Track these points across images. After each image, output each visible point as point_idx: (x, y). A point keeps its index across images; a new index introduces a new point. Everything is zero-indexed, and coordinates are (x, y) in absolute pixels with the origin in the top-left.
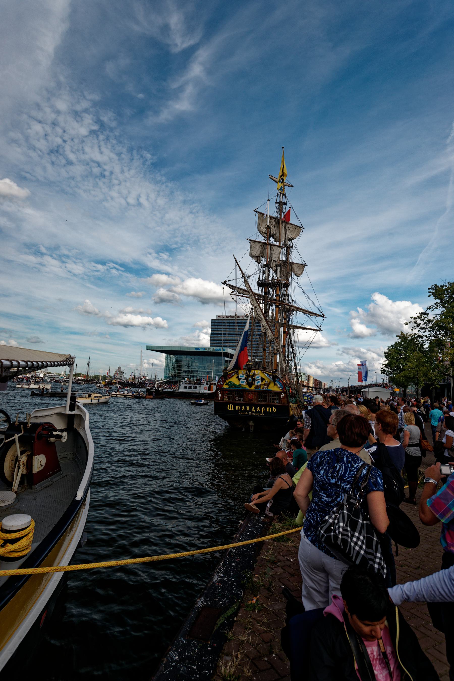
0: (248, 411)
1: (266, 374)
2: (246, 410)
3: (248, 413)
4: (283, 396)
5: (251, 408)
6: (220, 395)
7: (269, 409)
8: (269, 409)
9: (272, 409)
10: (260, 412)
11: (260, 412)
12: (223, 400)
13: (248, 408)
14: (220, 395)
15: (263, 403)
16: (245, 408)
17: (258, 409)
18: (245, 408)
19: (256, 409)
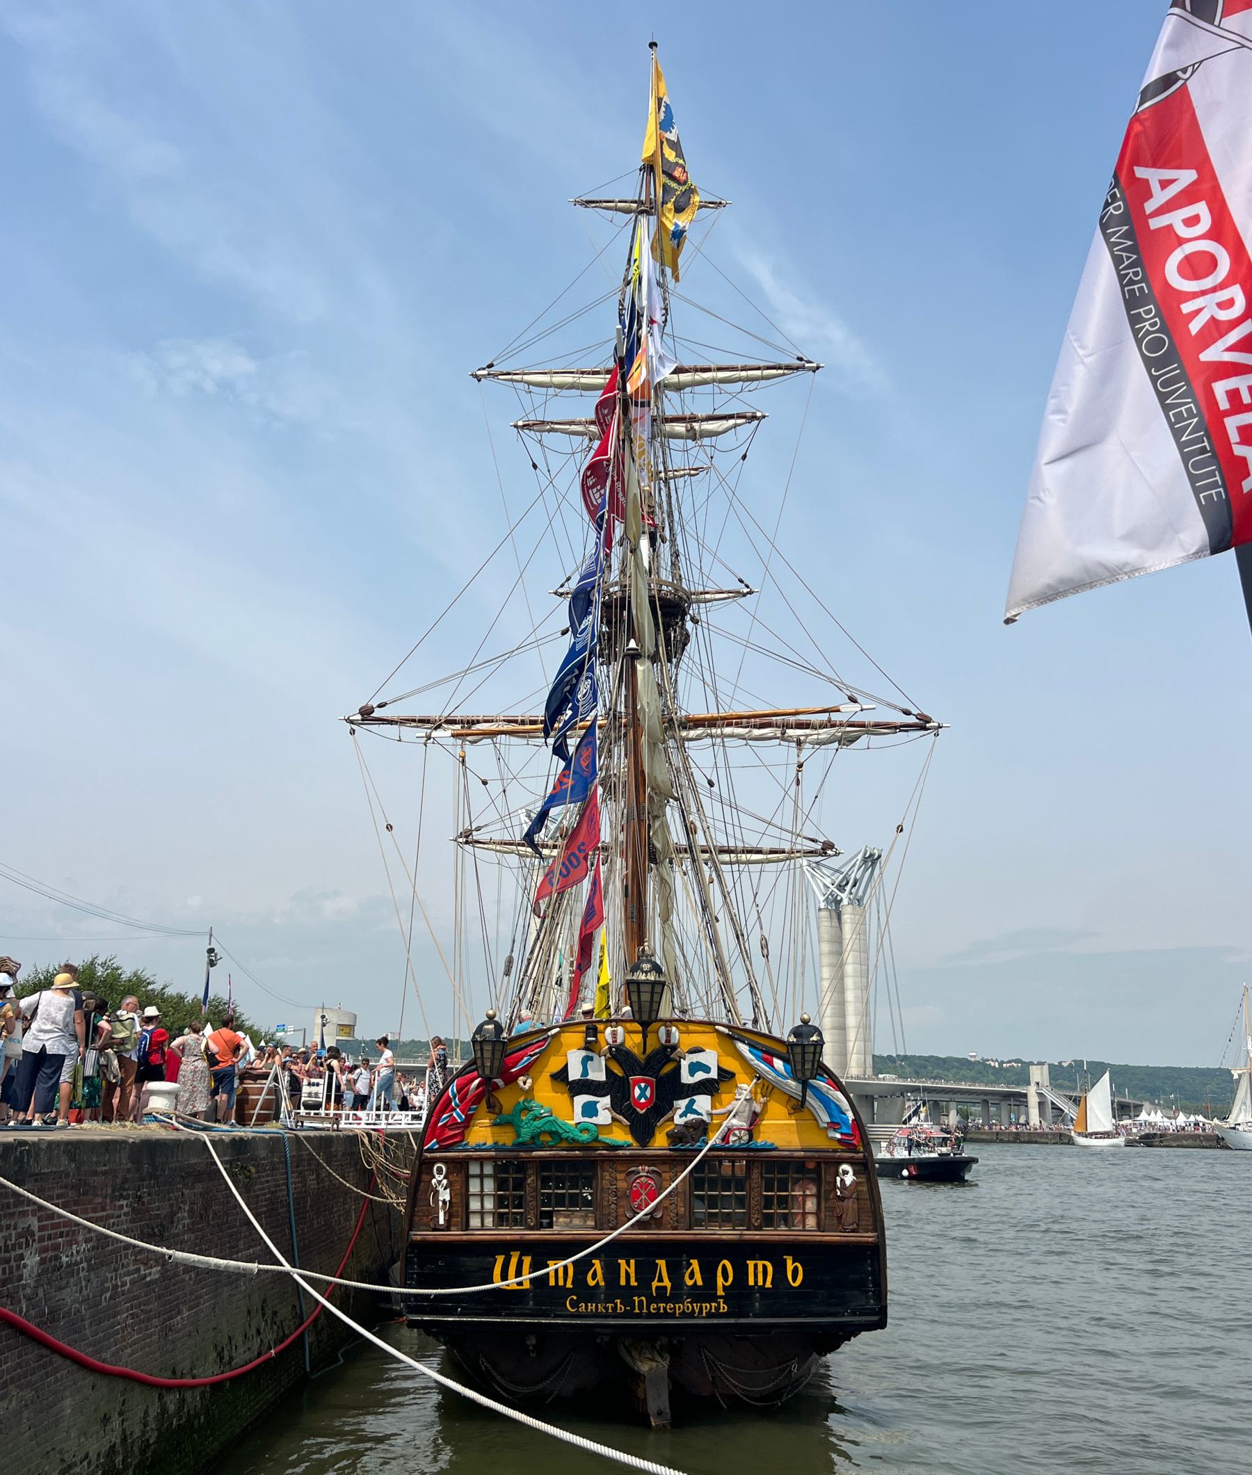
0: (627, 1294)
1: (743, 1048)
2: (613, 1287)
3: (628, 1302)
4: (849, 1179)
5: (646, 1272)
6: (445, 1195)
7: (759, 1273)
8: (759, 1273)
9: (780, 1268)
10: (705, 1293)
11: (705, 1293)
12: (466, 1226)
13: (627, 1269)
14: (445, 1195)
15: (726, 1233)
16: (612, 1272)
17: (694, 1274)
18: (612, 1272)
19: (676, 1272)
